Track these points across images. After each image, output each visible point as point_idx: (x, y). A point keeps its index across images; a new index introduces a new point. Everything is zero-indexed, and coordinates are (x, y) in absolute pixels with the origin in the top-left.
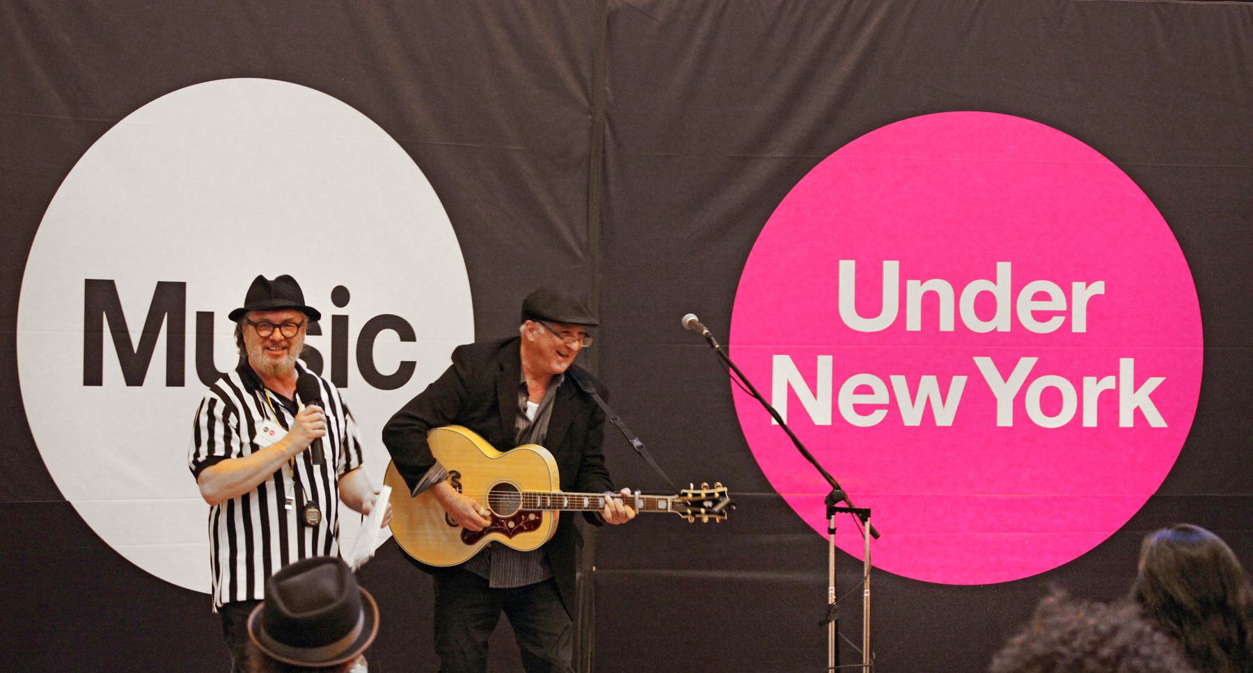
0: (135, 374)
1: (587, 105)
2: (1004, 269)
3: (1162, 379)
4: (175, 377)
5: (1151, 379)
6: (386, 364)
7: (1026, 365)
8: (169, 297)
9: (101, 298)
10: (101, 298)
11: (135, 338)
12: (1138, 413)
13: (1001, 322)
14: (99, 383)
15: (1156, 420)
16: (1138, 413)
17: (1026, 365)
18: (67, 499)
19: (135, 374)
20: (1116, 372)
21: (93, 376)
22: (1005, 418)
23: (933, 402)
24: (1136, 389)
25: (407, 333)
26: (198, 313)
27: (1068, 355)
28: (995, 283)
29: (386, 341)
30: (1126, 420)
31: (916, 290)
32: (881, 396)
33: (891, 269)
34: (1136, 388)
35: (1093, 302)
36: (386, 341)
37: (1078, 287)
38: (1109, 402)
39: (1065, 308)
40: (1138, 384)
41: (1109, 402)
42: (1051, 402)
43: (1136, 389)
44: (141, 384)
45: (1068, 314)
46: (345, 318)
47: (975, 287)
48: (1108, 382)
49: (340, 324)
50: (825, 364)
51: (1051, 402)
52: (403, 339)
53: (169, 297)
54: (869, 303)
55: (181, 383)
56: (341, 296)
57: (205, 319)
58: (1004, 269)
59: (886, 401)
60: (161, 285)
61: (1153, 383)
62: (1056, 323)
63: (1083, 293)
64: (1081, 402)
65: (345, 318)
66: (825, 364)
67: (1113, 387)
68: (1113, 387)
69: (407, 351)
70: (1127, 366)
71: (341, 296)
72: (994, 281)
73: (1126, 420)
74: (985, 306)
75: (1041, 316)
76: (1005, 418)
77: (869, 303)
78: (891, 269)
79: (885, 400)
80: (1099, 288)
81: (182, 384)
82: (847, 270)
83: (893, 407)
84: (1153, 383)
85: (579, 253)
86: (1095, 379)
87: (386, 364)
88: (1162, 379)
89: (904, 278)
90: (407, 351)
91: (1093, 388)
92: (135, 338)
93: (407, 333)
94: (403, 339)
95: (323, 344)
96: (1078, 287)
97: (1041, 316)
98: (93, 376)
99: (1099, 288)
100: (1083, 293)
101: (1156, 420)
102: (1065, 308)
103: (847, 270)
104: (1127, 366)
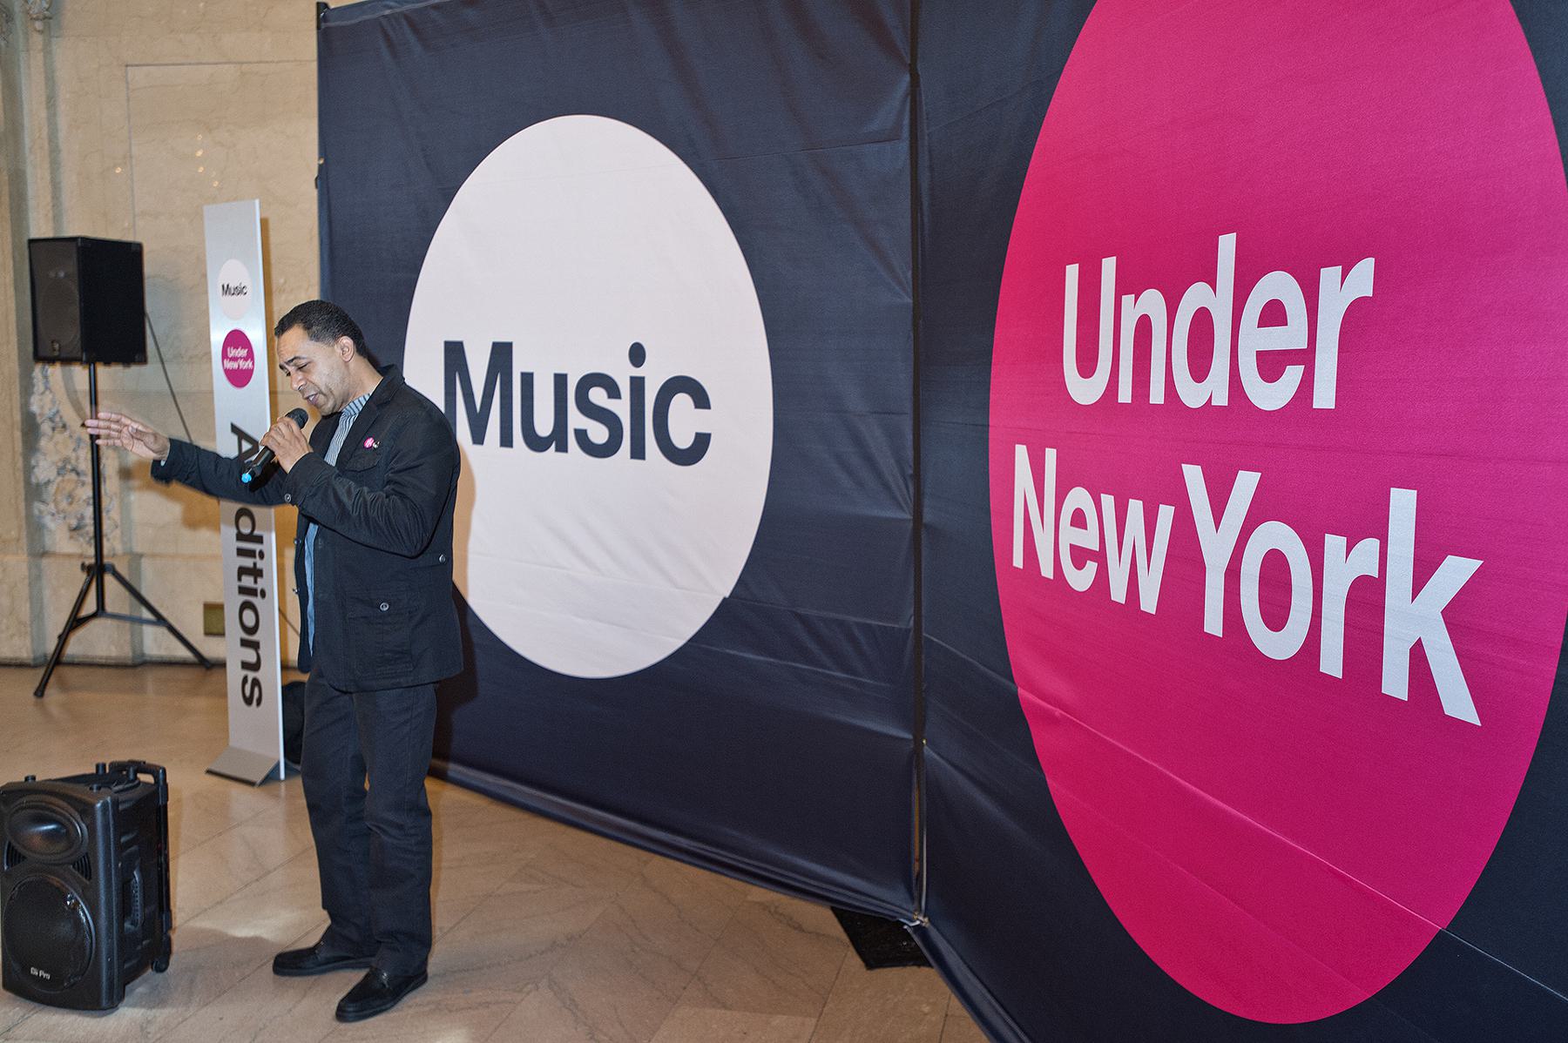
3: (1474, 565)
4: (506, 441)
5: (1451, 560)
6: (682, 439)
17: (1246, 484)
25: (701, 400)
29: (681, 403)
31: (1132, 310)
32: (1089, 540)
36: (681, 403)
37: (1329, 276)
46: (642, 379)
47: (1196, 296)
49: (638, 385)
52: (697, 406)
55: (511, 445)
56: (637, 355)
57: (528, 379)
59: (1096, 548)
61: (1456, 572)
65: (642, 379)
71: (637, 355)
75: (1271, 365)
79: (1094, 546)
83: (1100, 557)
84: (1456, 572)
86: (1342, 541)
88: (1474, 565)
89: (1121, 289)
93: (701, 400)
95: (621, 408)
97: (1271, 365)
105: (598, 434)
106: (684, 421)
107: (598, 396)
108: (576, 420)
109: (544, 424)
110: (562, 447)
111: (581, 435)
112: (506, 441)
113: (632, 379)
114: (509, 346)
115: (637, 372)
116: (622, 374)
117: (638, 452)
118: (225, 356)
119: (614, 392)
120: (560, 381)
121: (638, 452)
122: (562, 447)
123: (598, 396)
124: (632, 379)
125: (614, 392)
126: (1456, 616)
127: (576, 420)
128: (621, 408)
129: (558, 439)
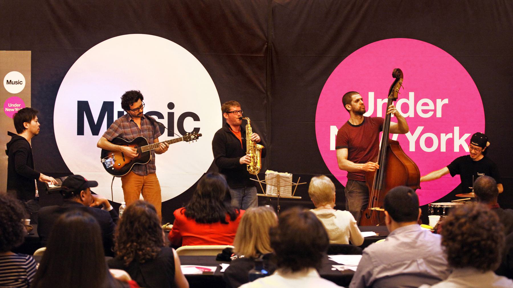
1: (266, 40)
2: (412, 95)
7: (420, 129)
9: (83, 107)
10: (83, 107)
11: (96, 120)
12: (461, 147)
13: (411, 114)
14: (83, 134)
16: (461, 147)
17: (420, 129)
19: (95, 131)
20: (453, 132)
22: (412, 148)
23: (13, 110)
24: (460, 138)
25: (196, 118)
27: (434, 125)
28: (408, 99)
30: (456, 149)
31: (380, 102)
33: (371, 95)
34: (461, 136)
35: (444, 106)
37: (439, 101)
38: (450, 143)
39: (433, 108)
40: (461, 136)
41: (450, 143)
42: (429, 142)
43: (460, 138)
45: (435, 111)
46: (173, 113)
48: (450, 135)
49: (171, 116)
51: (429, 142)
52: (195, 120)
56: (171, 106)
58: (412, 95)
60: (105, 103)
62: (431, 114)
63: (440, 103)
64: (440, 142)
67: (452, 137)
68: (452, 137)
69: (197, 124)
70: (457, 129)
71: (171, 106)
72: (408, 99)
73: (456, 149)
74: (405, 108)
75: (425, 112)
76: (412, 148)
78: (371, 95)
80: (446, 101)
85: (264, 91)
90: (197, 124)
91: (444, 138)
92: (96, 120)
93: (196, 118)
95: (165, 122)
96: (439, 101)
97: (425, 112)
98: (81, 131)
99: (446, 101)
100: (440, 103)
102: (433, 108)
104: (457, 129)
106: (189, 125)
113: (169, 113)
116: (165, 112)
119: (161, 116)
124: (169, 113)
126: (466, 140)
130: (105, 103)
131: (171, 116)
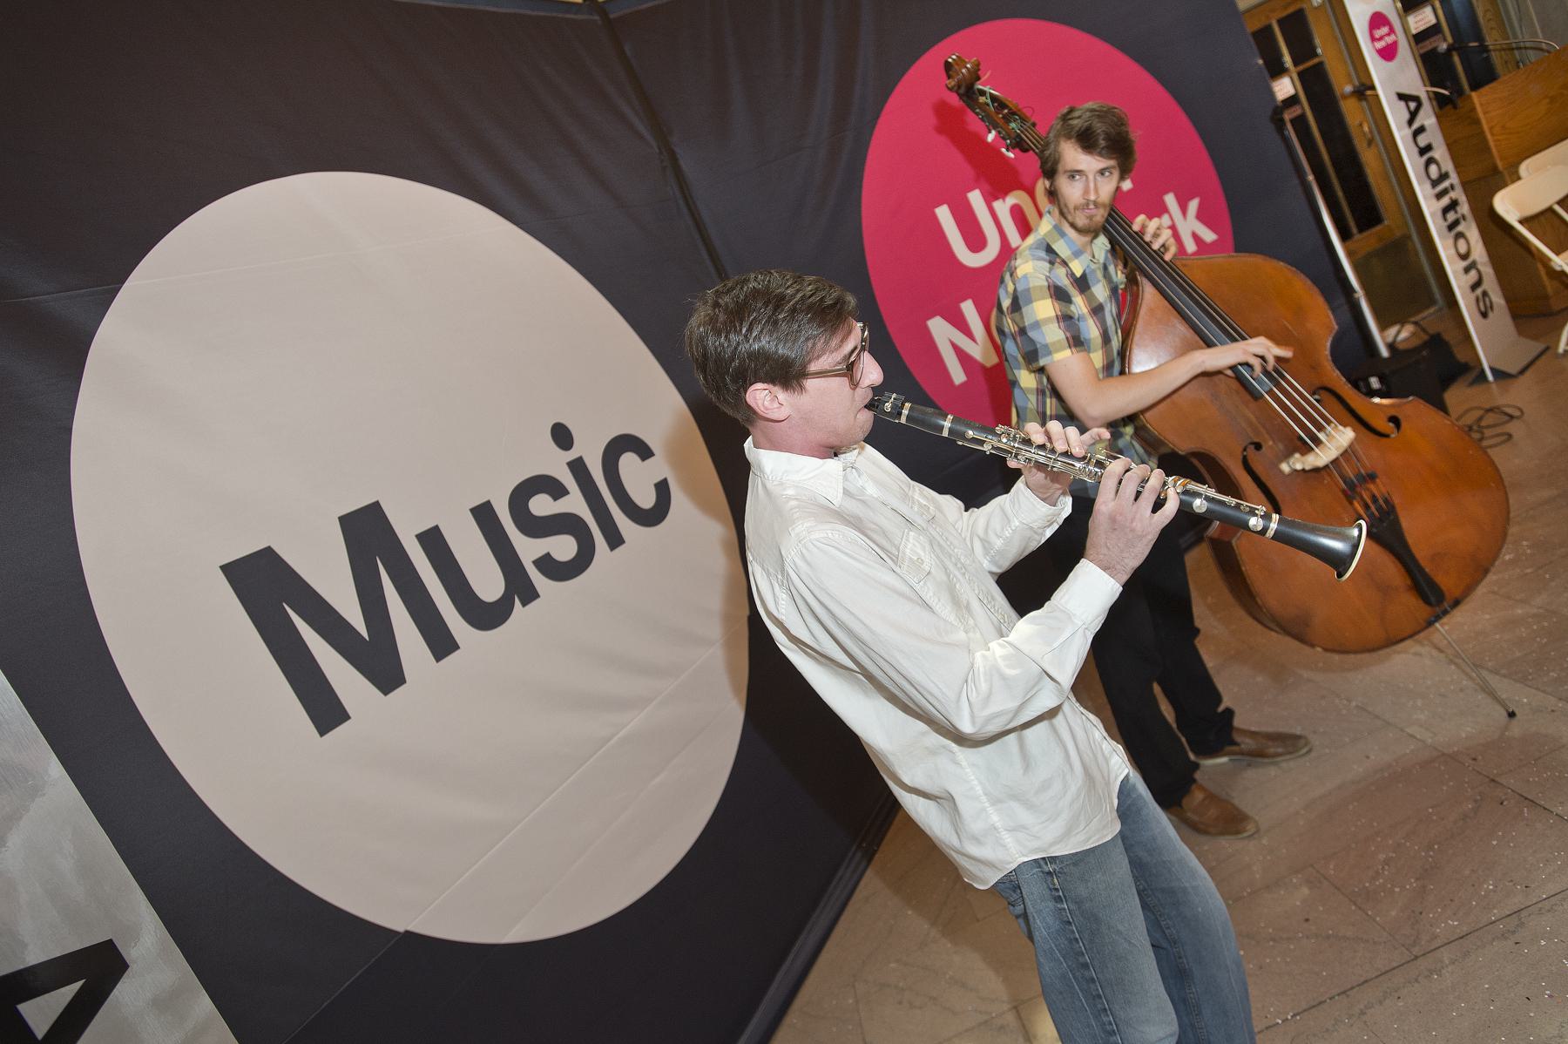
0: (384, 670)
4: (442, 644)
6: (645, 498)
8: (367, 533)
9: (264, 584)
10: (264, 584)
11: (354, 616)
12: (1195, 237)
15: (1209, 236)
18: (400, 927)
19: (384, 670)
21: (326, 711)
25: (645, 452)
26: (419, 537)
31: (1003, 207)
33: (976, 198)
34: (1184, 210)
40: (1184, 210)
44: (402, 681)
46: (580, 460)
49: (578, 468)
50: (968, 308)
52: (643, 459)
53: (367, 533)
54: (976, 241)
55: (455, 647)
56: (562, 436)
57: (433, 541)
60: (346, 522)
61: (1194, 205)
65: (580, 460)
66: (968, 308)
70: (1170, 200)
71: (562, 436)
77: (976, 241)
78: (976, 198)
81: (455, 647)
82: (943, 214)
84: (1194, 205)
87: (645, 498)
89: (990, 198)
92: (354, 616)
93: (645, 452)
94: (643, 459)
95: (575, 503)
98: (326, 711)
101: (1209, 236)
103: (943, 214)
104: (1170, 200)
105: (563, 547)
106: (639, 478)
107: (541, 505)
108: (528, 549)
109: (488, 582)
110: (529, 595)
111: (548, 565)
112: (442, 644)
113: (570, 464)
114: (375, 510)
115: (572, 455)
116: (556, 464)
117: (615, 540)
118: (1373, 39)
119: (557, 490)
120: (484, 515)
121: (615, 540)
122: (529, 595)
123: (541, 505)
124: (570, 464)
125: (557, 490)
127: (528, 549)
128: (575, 503)
129: (520, 588)
130: (346, 522)
131: (578, 468)
